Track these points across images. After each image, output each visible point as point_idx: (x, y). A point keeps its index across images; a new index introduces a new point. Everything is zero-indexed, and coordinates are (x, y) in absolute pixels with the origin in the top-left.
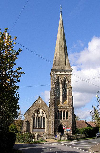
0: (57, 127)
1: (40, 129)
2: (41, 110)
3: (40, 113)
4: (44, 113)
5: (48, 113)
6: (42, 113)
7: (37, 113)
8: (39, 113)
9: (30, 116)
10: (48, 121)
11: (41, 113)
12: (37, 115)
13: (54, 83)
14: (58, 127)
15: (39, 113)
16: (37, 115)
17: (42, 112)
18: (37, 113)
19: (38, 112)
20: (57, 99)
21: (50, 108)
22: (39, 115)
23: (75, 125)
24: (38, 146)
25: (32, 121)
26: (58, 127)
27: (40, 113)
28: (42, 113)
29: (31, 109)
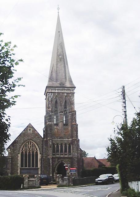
0: (56, 166)
1: (31, 169)
2: (32, 143)
3: (31, 147)
4: (37, 147)
5: (43, 147)
6: (34, 147)
7: (27, 147)
8: (29, 147)
9: (15, 150)
10: (42, 157)
11: (32, 147)
12: (27, 149)
13: (50, 105)
14: (57, 166)
15: (29, 147)
16: (27, 149)
17: (34, 145)
18: (27, 147)
19: (28, 145)
20: (55, 127)
21: (45, 139)
22: (30, 149)
23: (81, 164)
24: (126, 122)
25: (19, 158)
26: (57, 166)
27: (31, 147)
28: (34, 147)
29: (17, 141)
